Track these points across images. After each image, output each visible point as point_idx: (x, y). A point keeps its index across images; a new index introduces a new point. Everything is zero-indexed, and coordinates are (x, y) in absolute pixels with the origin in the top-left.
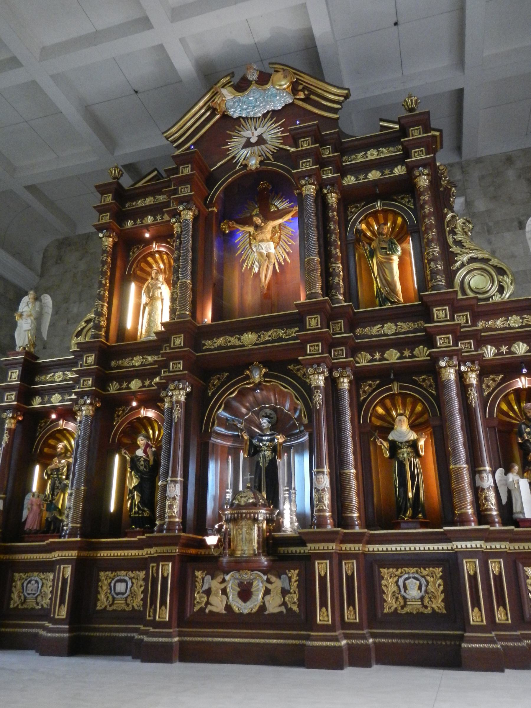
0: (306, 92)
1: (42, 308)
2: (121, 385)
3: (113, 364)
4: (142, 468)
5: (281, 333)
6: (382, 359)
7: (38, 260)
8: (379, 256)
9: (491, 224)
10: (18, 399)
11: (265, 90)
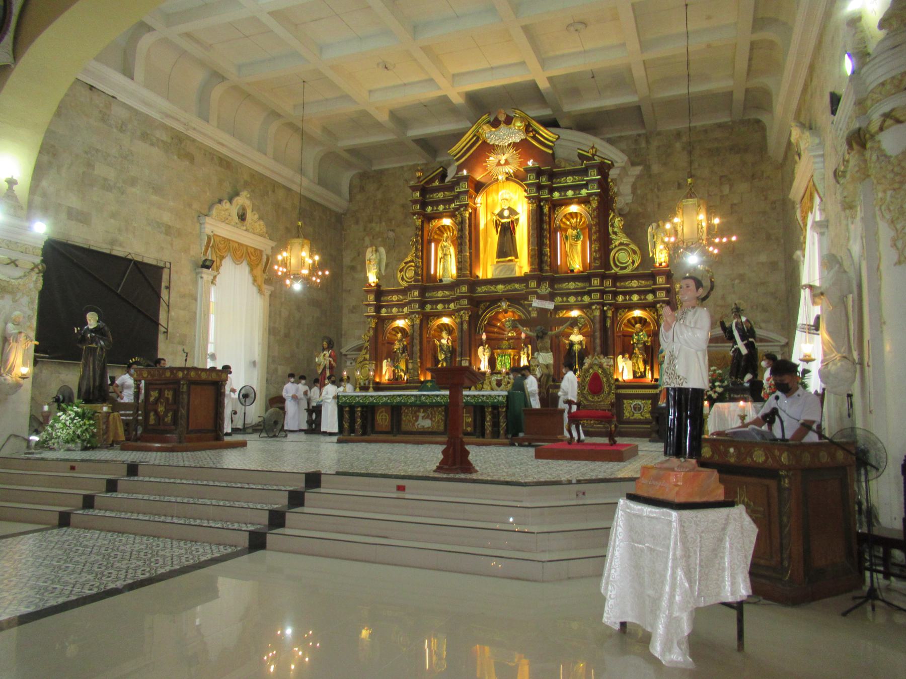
0: (534, 133)
1: (380, 255)
2: (432, 306)
3: (427, 295)
4: (445, 350)
5: (517, 286)
6: (567, 301)
7: (345, 189)
8: (571, 241)
9: (660, 184)
10: (375, 311)
11: (510, 128)
